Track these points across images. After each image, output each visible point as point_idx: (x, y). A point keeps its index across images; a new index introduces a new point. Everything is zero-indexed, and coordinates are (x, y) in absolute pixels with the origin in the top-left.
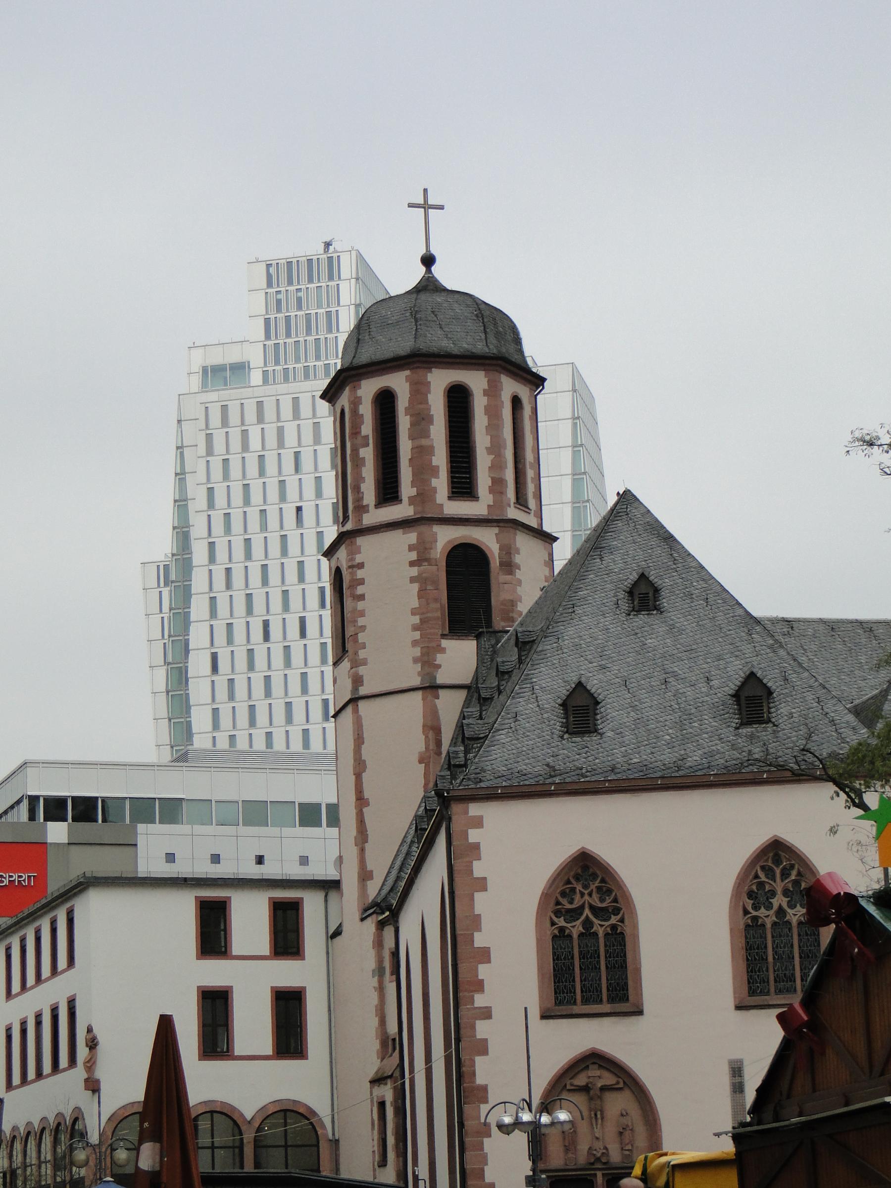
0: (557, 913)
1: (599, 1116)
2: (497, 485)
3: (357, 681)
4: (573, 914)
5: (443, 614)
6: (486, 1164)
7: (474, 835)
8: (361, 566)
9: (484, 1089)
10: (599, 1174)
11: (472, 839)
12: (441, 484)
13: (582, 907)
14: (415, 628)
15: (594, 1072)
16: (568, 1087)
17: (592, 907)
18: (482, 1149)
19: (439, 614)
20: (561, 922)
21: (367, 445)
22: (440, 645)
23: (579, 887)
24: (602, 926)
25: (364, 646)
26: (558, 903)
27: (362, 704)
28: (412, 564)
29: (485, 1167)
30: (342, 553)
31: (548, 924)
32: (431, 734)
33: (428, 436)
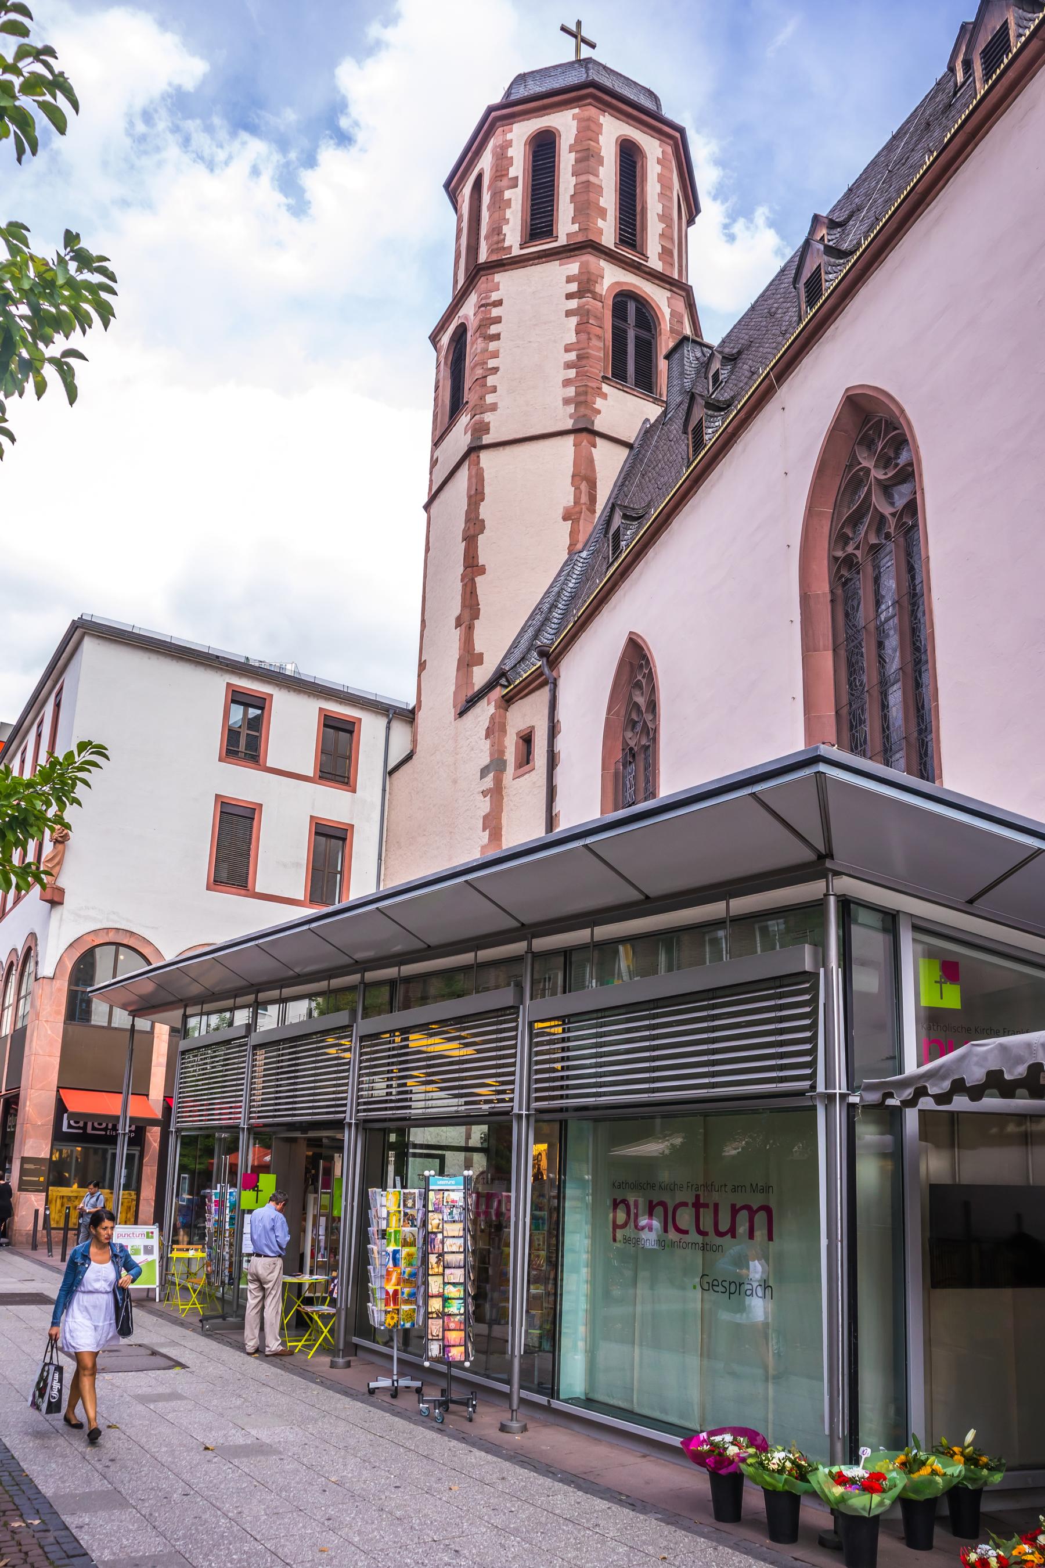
3: (482, 429)
5: (606, 355)
8: (499, 303)
22: (600, 389)
27: (486, 458)
28: (569, 296)
32: (584, 486)
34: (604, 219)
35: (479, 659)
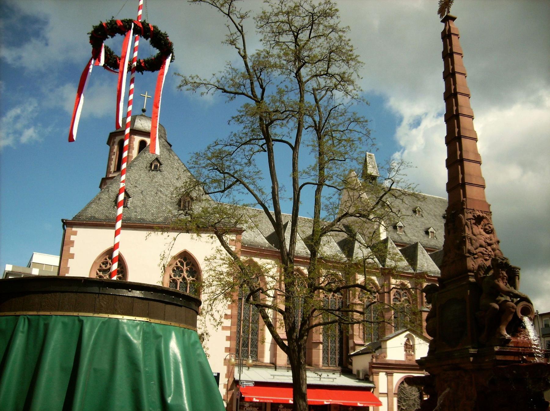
7: (73, 238)
11: (72, 239)
20: (101, 274)
26: (101, 267)
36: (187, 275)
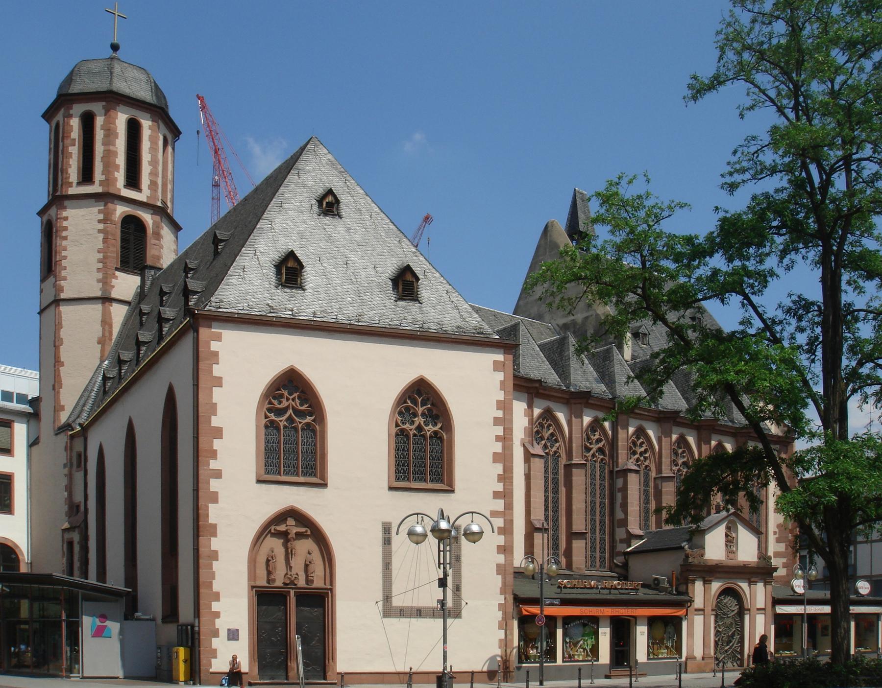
0: (270, 410)
1: (293, 552)
2: (153, 185)
4: (280, 412)
5: (117, 254)
6: (215, 579)
9: (214, 526)
10: (292, 592)
12: (120, 177)
13: (287, 408)
14: (99, 261)
15: (291, 522)
16: (273, 531)
17: (293, 408)
18: (212, 569)
19: (115, 255)
20: (272, 416)
21: (74, 145)
22: (114, 274)
23: (286, 393)
24: (300, 423)
25: (65, 268)
28: (100, 221)
29: (213, 581)
30: (53, 211)
31: (264, 417)
33: (114, 145)
34: (118, 172)
35: (62, 408)
36: (425, 422)
